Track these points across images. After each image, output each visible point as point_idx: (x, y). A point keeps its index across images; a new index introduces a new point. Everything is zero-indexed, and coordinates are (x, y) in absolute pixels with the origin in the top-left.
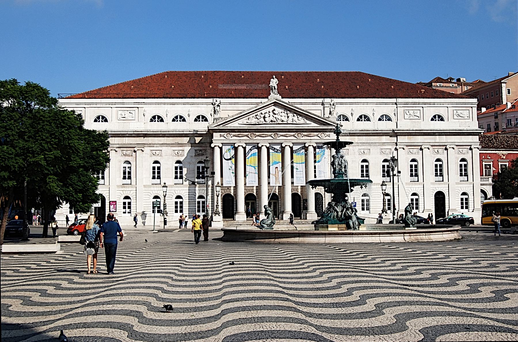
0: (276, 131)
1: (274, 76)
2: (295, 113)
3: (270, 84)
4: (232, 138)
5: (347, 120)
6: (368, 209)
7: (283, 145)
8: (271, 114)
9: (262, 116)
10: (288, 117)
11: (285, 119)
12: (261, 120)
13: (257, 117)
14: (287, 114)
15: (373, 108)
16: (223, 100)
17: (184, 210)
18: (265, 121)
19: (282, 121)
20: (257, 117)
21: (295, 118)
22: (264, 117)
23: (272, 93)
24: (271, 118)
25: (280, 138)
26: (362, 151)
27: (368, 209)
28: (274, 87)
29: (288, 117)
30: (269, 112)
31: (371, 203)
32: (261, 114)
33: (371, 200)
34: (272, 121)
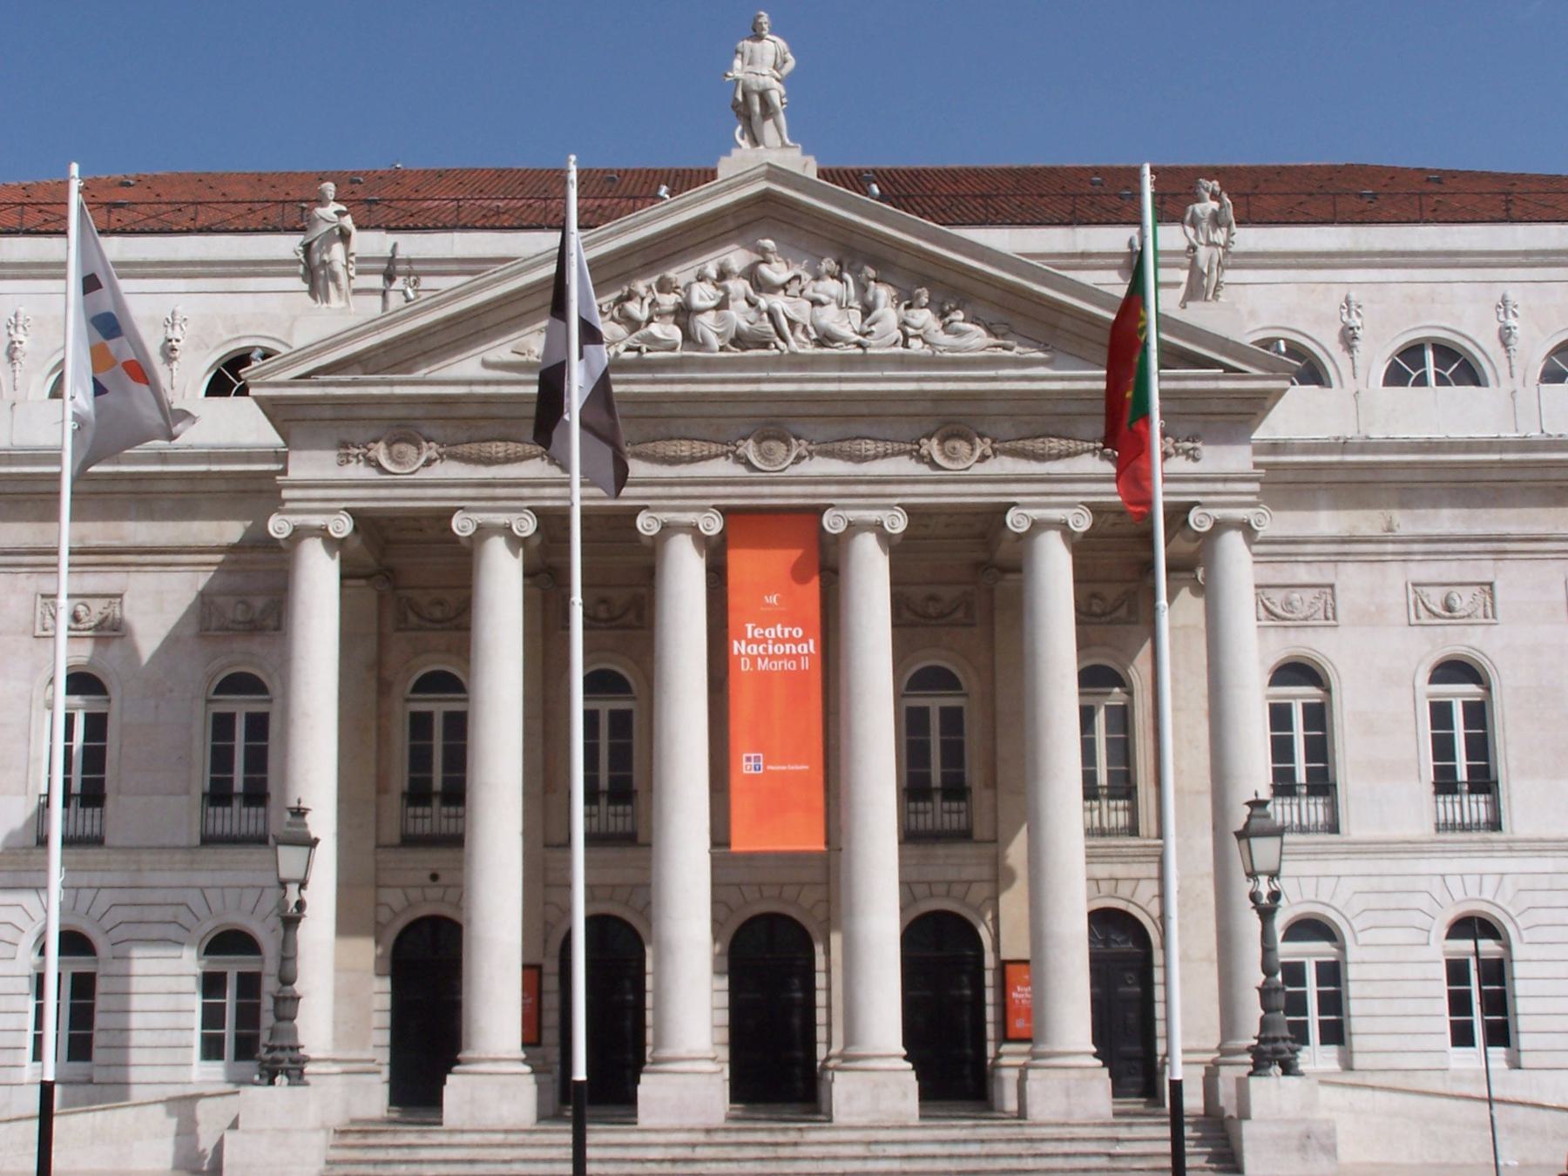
0: (775, 422)
1: (765, 18)
2: (925, 281)
3: (730, 67)
4: (428, 478)
5: (1312, 372)
6: (1500, 1035)
7: (833, 523)
8: (738, 286)
9: (669, 301)
10: (868, 310)
11: (845, 324)
12: (656, 329)
13: (633, 308)
14: (862, 288)
15: (1498, 291)
16: (413, 245)
17: (99, 1039)
18: (688, 337)
19: (826, 338)
20: (633, 308)
21: (923, 317)
22: (684, 314)
23: (745, 144)
24: (739, 316)
25: (806, 473)
26: (1435, 597)
27: (1500, 1035)
28: (764, 96)
29: (868, 310)
30: (723, 274)
31: (1520, 987)
32: (664, 286)
33: (1519, 969)
34: (740, 340)
